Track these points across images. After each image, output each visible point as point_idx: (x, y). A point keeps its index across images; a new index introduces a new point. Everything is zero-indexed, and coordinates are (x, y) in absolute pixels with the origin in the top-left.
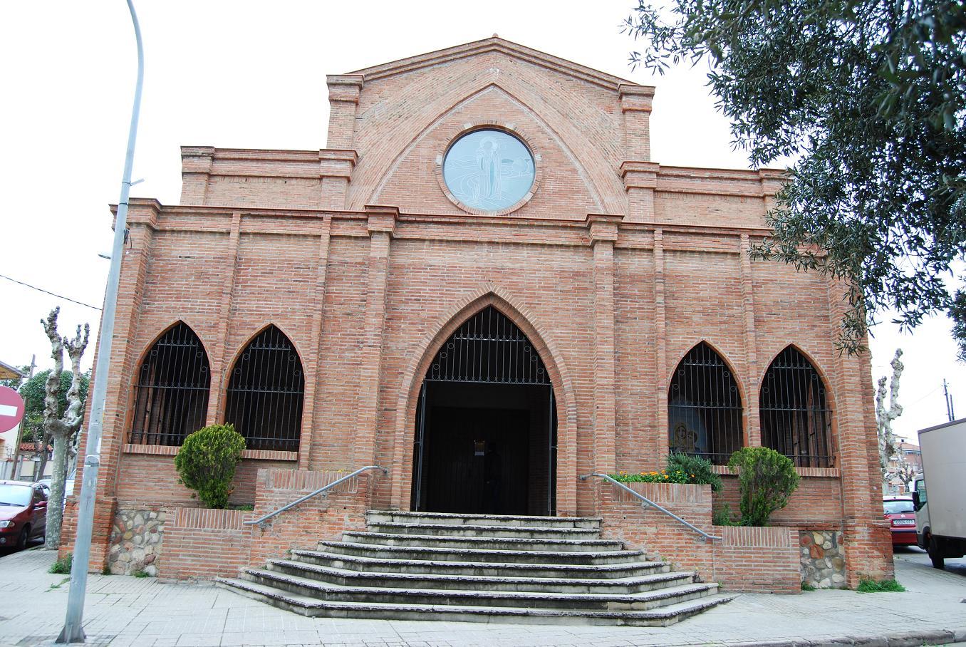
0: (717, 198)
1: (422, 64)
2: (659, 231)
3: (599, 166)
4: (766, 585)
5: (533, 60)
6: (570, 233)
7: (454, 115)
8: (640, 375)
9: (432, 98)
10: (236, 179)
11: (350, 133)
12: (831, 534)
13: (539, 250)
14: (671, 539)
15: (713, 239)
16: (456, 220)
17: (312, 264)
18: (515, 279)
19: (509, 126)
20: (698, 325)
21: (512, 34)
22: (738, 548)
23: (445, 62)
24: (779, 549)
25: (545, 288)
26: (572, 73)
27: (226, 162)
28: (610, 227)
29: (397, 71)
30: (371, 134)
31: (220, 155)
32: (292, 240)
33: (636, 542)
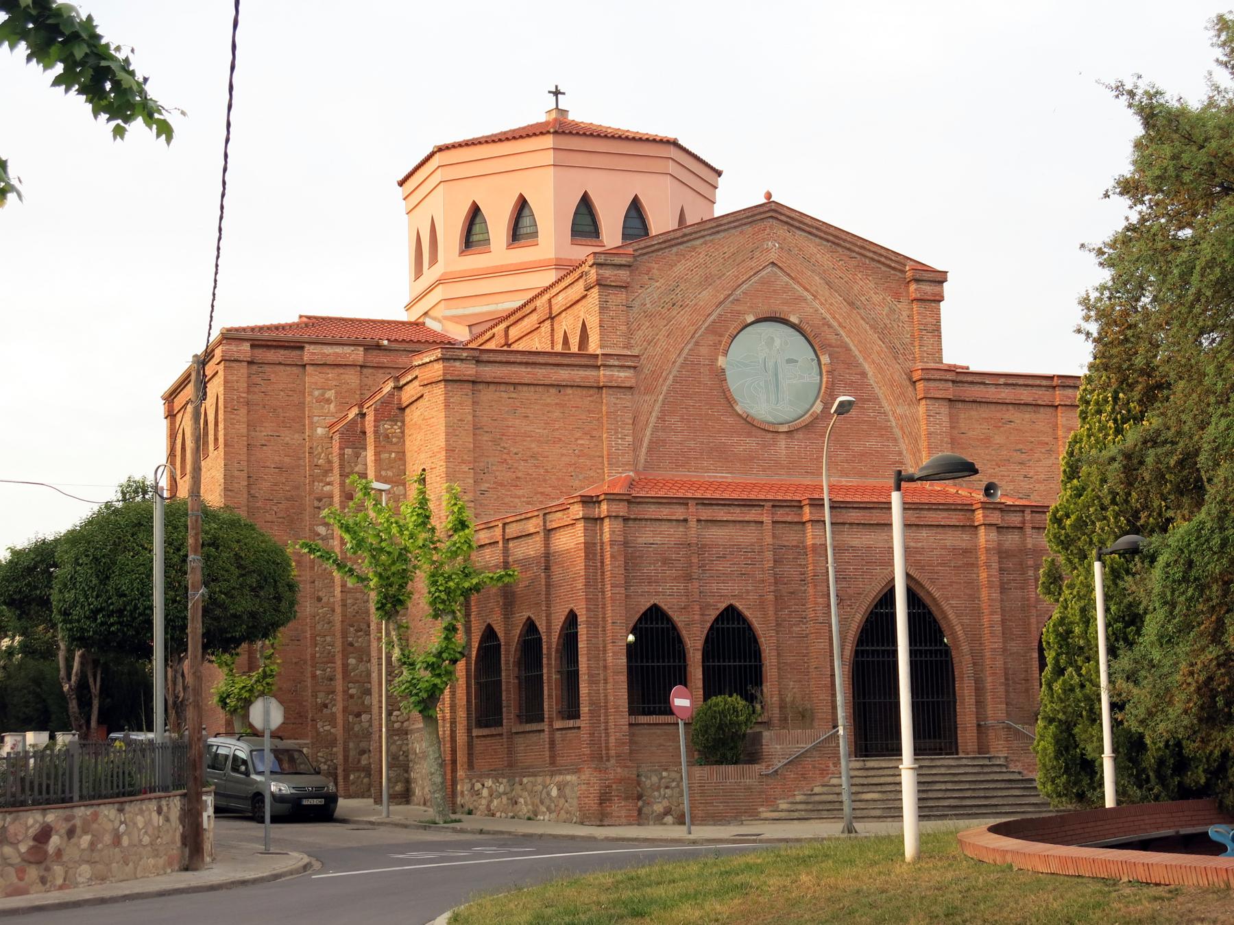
0: (1010, 407)
1: (694, 236)
2: (1028, 511)
5: (814, 231)
7: (732, 302)
9: (707, 281)
10: (503, 388)
11: (624, 328)
13: (935, 530)
16: (871, 506)
17: (757, 548)
19: (794, 319)
21: (791, 198)
23: (718, 232)
26: (857, 249)
29: (667, 244)
30: (644, 328)
31: (485, 357)
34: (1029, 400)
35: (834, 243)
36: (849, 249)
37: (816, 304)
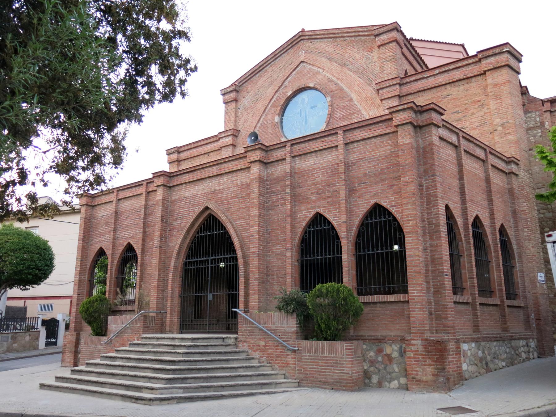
0: (448, 86)
1: (265, 65)
3: (366, 91)
4: (329, 384)
5: (323, 36)
6: (244, 161)
7: (283, 89)
8: (281, 242)
10: (189, 160)
12: (398, 346)
13: (231, 175)
14: (272, 349)
15: (322, 140)
16: (192, 169)
18: (220, 195)
19: (311, 85)
20: (314, 202)
21: (311, 26)
22: (311, 356)
23: (277, 58)
24: (337, 357)
25: (234, 197)
26: (345, 35)
27: (184, 152)
28: (256, 152)
30: (244, 116)
31: (181, 150)
32: (136, 198)
33: (254, 351)
34: (461, 76)
35: (334, 37)
36: (342, 37)
37: (325, 73)
